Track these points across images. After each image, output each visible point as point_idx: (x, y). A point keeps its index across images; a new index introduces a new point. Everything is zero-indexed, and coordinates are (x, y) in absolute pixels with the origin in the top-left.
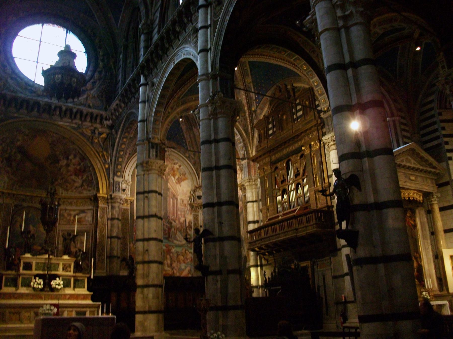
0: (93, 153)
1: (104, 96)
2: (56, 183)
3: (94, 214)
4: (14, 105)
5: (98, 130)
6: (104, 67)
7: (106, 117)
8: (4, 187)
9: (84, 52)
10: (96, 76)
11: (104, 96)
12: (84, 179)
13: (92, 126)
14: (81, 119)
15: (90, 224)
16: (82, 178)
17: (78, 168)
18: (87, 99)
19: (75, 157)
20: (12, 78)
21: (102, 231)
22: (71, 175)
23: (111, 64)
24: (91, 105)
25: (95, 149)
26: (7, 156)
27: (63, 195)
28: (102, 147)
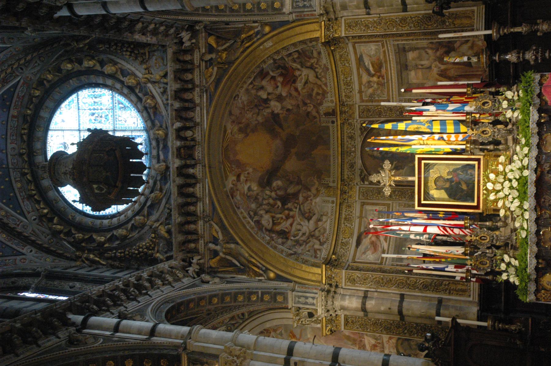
0: (248, 60)
1: (142, 51)
2: (314, 113)
3: (362, 40)
4: (192, 208)
5: (203, 54)
6: (93, 58)
7: (176, 43)
8: (333, 202)
9: (78, 96)
10: (109, 69)
11: (142, 51)
12: (299, 67)
13: (199, 66)
14: (192, 90)
15: (383, 46)
16: (298, 70)
17: (280, 79)
18: (154, 83)
19: (262, 88)
20: (149, 214)
21: (392, 22)
22: (296, 90)
23: (81, 46)
24: (162, 74)
25: (238, 58)
26: (279, 203)
27: (334, 99)
28: (234, 42)
